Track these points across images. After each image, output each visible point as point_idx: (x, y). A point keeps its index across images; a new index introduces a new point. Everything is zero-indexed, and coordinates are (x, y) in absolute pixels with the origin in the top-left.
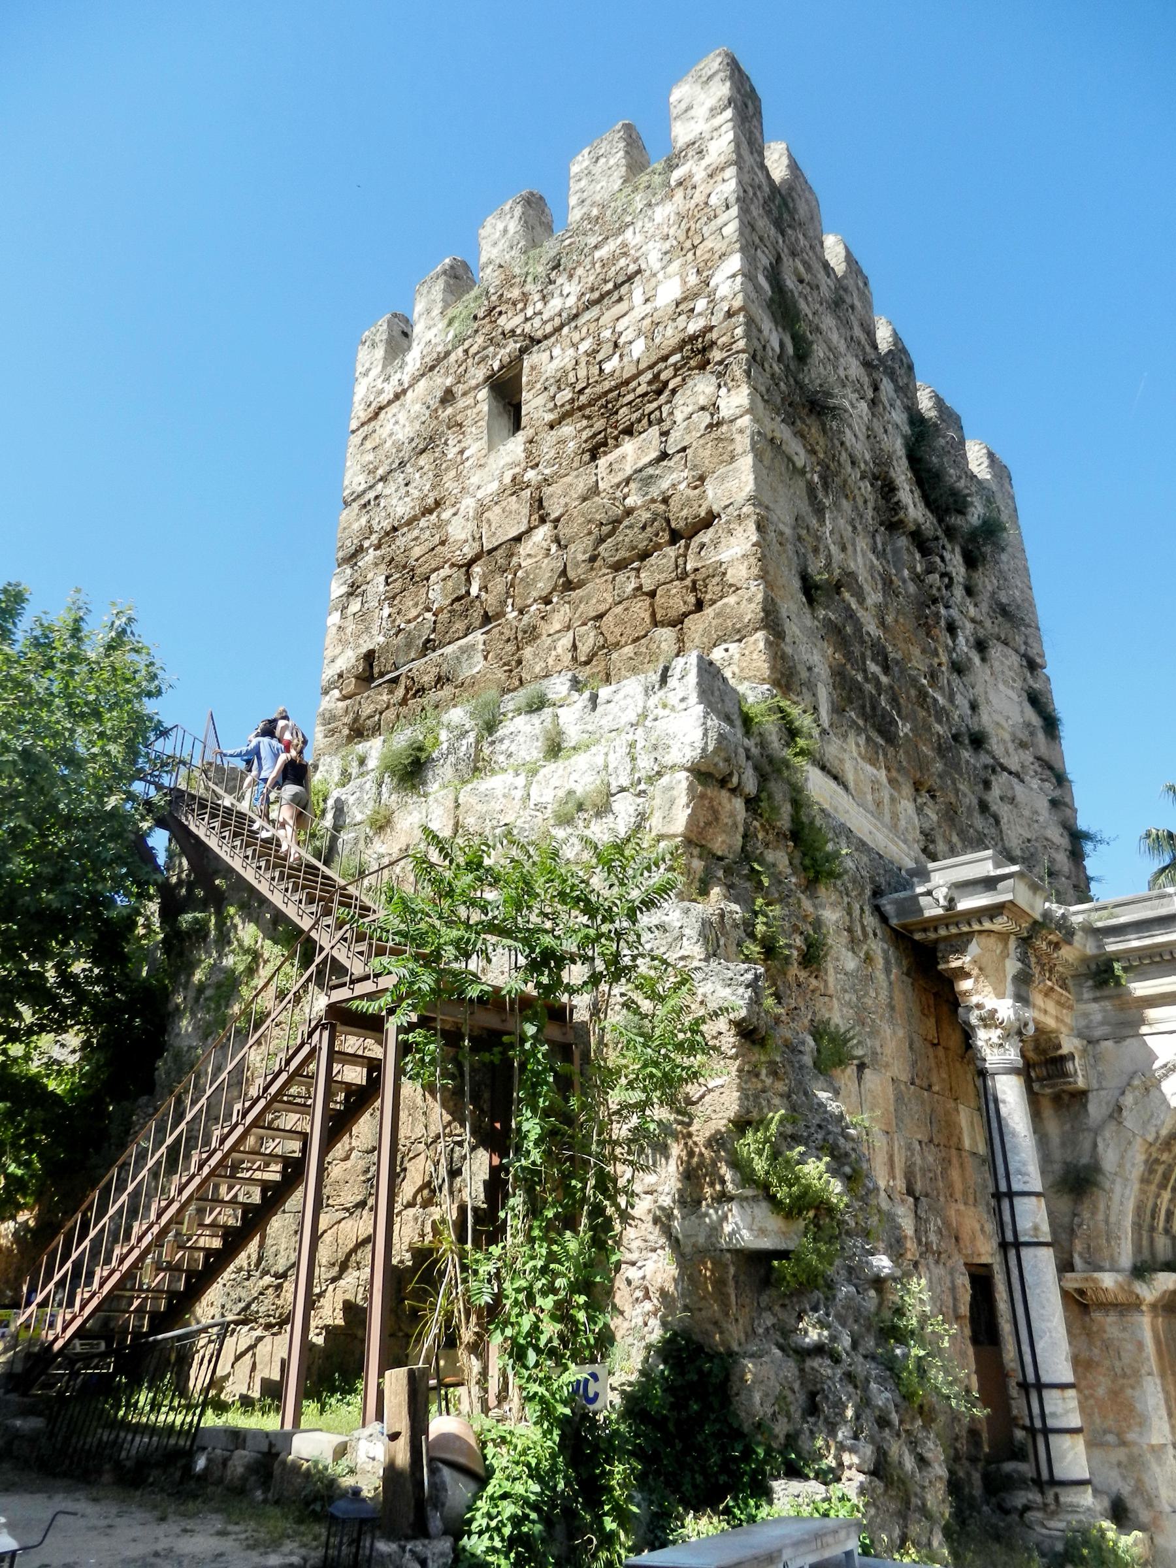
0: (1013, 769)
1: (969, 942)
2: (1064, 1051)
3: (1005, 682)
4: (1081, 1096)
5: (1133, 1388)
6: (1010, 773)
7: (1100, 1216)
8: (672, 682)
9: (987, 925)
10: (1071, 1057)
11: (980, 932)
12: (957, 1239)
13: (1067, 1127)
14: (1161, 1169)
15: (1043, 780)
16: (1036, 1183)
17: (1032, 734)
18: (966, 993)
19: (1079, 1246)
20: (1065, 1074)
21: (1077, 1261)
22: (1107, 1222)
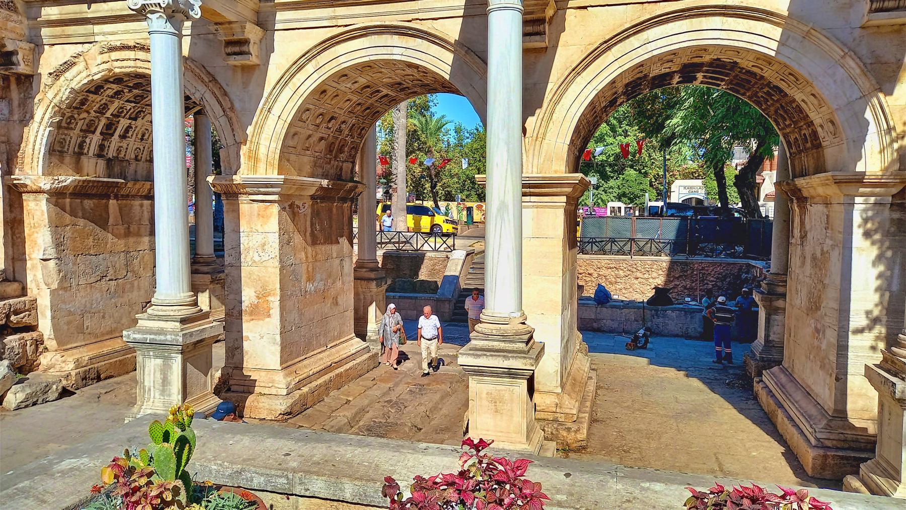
2: (10, 47)
5: (37, 233)
13: (22, 95)
20: (13, 64)
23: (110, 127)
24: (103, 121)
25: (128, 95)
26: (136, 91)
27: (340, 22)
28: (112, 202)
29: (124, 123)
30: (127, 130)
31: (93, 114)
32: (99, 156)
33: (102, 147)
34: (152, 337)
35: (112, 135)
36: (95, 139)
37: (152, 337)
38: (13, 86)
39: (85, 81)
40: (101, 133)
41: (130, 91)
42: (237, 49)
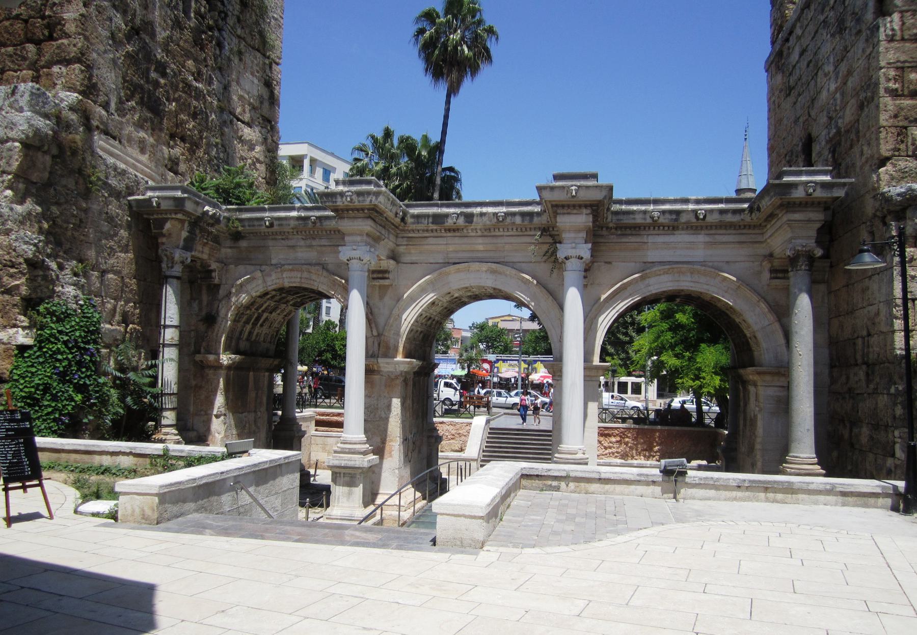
0: (246, 120)
1: (167, 222)
3: (252, 74)
4: (218, 286)
6: (243, 122)
7: (214, 334)
8: (17, 96)
9: (174, 216)
10: (214, 271)
11: (173, 218)
12: (148, 340)
13: (210, 298)
14: (245, 317)
15: (262, 127)
16: (176, 322)
17: (261, 103)
18: (163, 244)
19: (204, 344)
20: (212, 278)
21: (202, 350)
22: (217, 336)
23: (258, 319)
24: (256, 315)
25: (277, 298)
26: (284, 295)
27: (451, 261)
28: (251, 373)
29: (265, 315)
30: (264, 321)
31: (253, 309)
32: (247, 340)
33: (250, 333)
34: (346, 462)
35: (257, 324)
36: (249, 327)
37: (346, 462)
38: (204, 291)
39: (262, 290)
40: (253, 324)
41: (280, 295)
42: (380, 275)
